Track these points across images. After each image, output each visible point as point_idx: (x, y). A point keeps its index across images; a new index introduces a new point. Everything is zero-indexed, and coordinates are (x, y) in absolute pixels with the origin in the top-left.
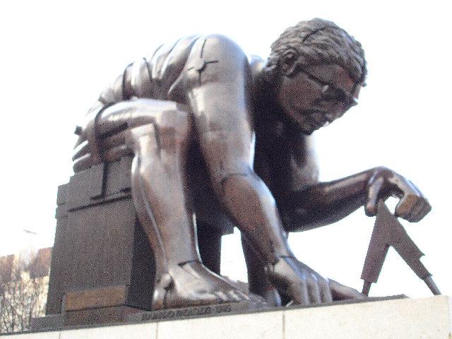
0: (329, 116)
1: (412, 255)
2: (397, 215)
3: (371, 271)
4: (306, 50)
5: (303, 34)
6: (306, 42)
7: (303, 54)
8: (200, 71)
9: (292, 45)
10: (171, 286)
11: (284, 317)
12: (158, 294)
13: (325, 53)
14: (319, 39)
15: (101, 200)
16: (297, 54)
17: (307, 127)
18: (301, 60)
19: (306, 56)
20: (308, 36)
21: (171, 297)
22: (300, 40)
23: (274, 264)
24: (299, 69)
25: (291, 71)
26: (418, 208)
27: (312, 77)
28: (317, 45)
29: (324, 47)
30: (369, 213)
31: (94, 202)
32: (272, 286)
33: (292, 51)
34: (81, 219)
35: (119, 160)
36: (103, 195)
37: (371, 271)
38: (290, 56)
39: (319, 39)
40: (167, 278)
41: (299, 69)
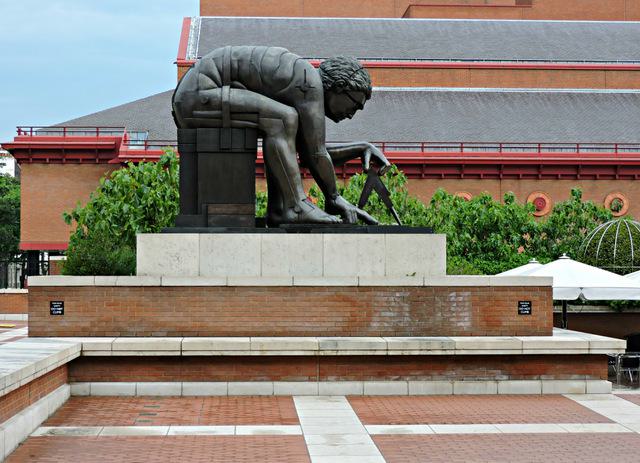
4: (352, 83)
16: (347, 83)
21: (302, 217)
27: (350, 96)
29: (359, 82)
39: (358, 77)
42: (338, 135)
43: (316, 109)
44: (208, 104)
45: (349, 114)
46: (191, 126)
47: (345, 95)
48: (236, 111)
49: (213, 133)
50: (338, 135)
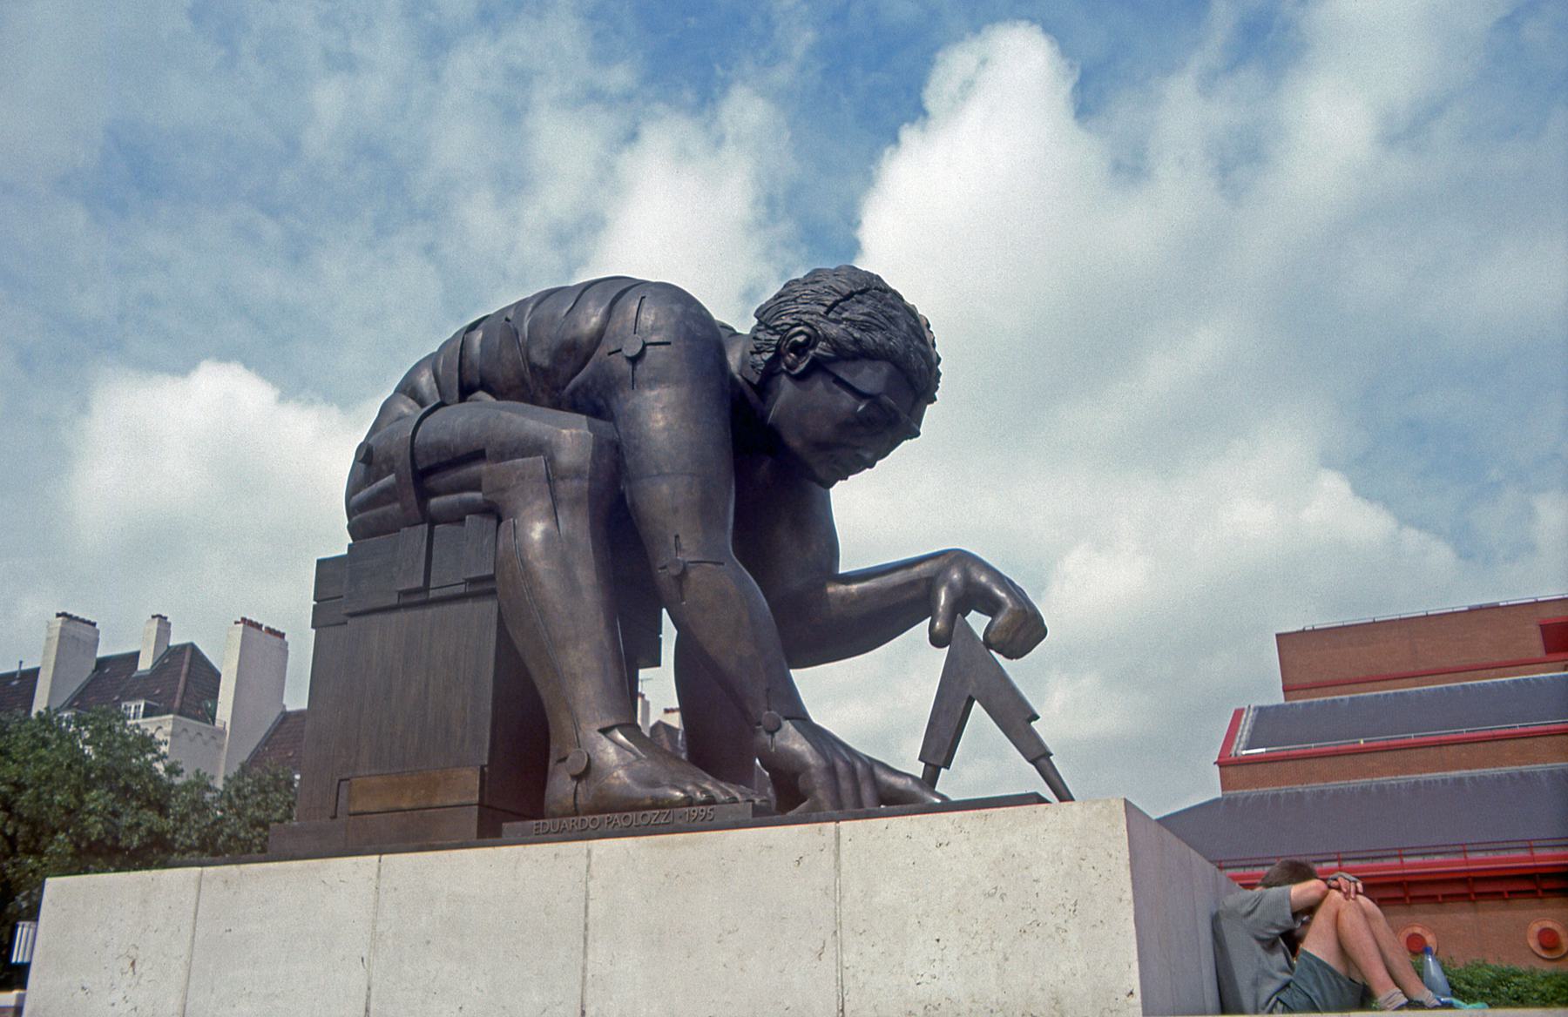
0: (868, 456)
1: (1016, 719)
2: (988, 644)
3: (941, 744)
4: (834, 331)
5: (829, 300)
6: (831, 315)
7: (826, 338)
8: (634, 360)
9: (806, 318)
10: (585, 773)
11: (838, 837)
12: (561, 786)
13: (866, 337)
14: (858, 311)
15: (422, 597)
17: (821, 472)
18: (821, 349)
19: (835, 344)
20: (836, 303)
21: (585, 793)
22: (822, 310)
23: (772, 733)
24: (817, 366)
25: (802, 367)
26: (1024, 631)
28: (852, 322)
30: (937, 640)
31: (404, 600)
32: (742, 761)
33: (807, 330)
34: (384, 636)
35: (461, 520)
36: (426, 587)
37: (941, 744)
38: (800, 339)
40: (576, 763)
41: (817, 366)
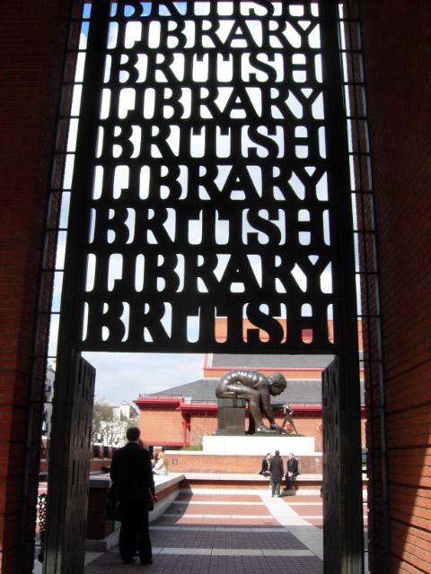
42: (275, 400)
43: (264, 392)
44: (228, 390)
45: (279, 394)
46: (222, 397)
47: (280, 386)
48: (237, 393)
49: (231, 400)
50: (275, 400)
